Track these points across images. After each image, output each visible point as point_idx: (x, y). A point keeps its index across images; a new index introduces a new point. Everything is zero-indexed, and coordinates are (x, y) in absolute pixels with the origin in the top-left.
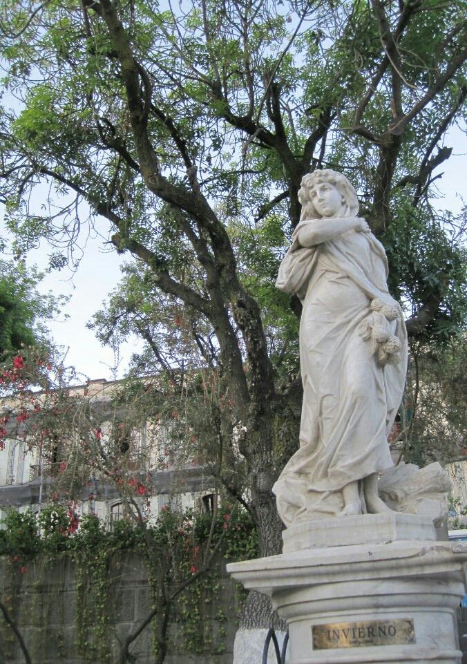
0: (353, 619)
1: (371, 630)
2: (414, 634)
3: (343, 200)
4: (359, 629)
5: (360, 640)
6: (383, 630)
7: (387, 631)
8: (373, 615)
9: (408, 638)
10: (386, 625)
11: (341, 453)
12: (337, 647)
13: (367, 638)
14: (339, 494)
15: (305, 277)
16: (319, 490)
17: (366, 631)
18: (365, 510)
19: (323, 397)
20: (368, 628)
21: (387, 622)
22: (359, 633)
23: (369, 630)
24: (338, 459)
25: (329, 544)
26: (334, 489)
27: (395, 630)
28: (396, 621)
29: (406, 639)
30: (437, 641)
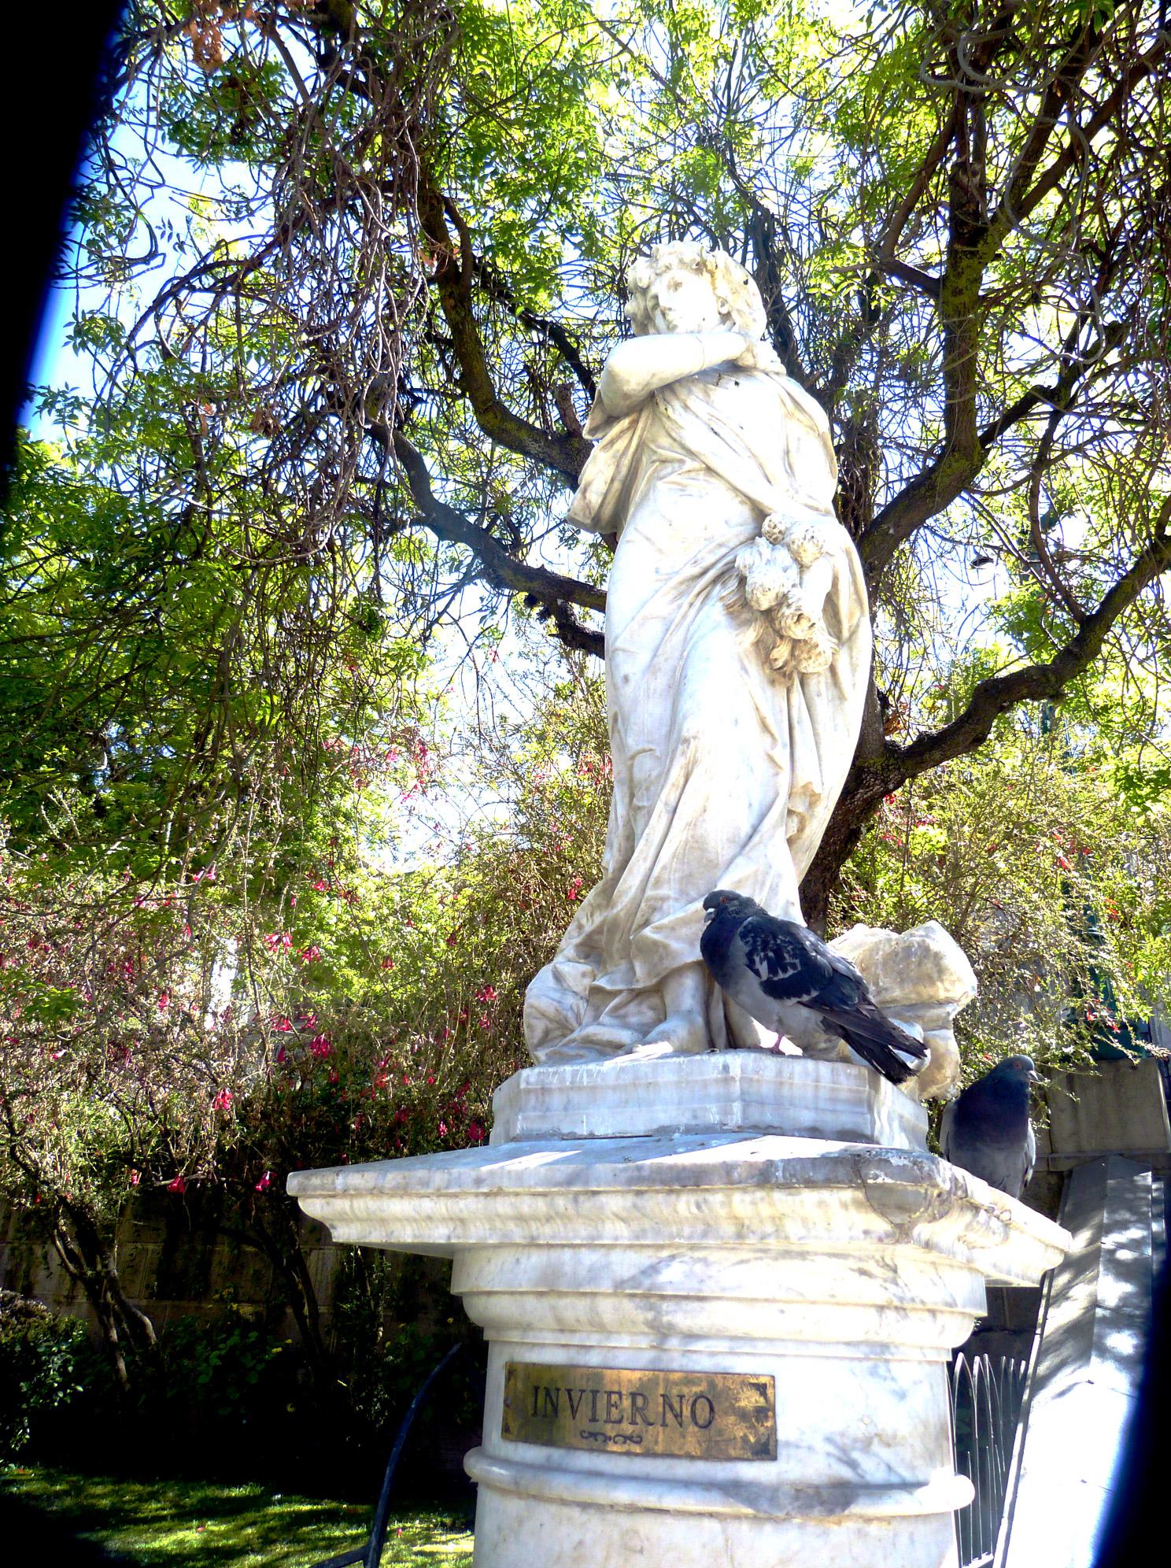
0: (594, 1359)
1: (640, 1401)
2: (773, 1430)
3: (724, 311)
4: (610, 1393)
5: (610, 1430)
6: (676, 1406)
7: (687, 1412)
8: (652, 1354)
9: (752, 1439)
10: (685, 1390)
11: (664, 891)
12: (549, 1442)
13: (627, 1428)
14: (655, 1000)
15: (617, 485)
16: (608, 987)
17: (626, 1403)
18: (721, 1040)
19: (633, 758)
20: (634, 1395)
21: (690, 1378)
22: (610, 1405)
23: (634, 1403)
24: (654, 909)
25: (565, 1130)
26: (640, 986)
27: (712, 1409)
28: (719, 1382)
29: (745, 1439)
30: (856, 1455)
